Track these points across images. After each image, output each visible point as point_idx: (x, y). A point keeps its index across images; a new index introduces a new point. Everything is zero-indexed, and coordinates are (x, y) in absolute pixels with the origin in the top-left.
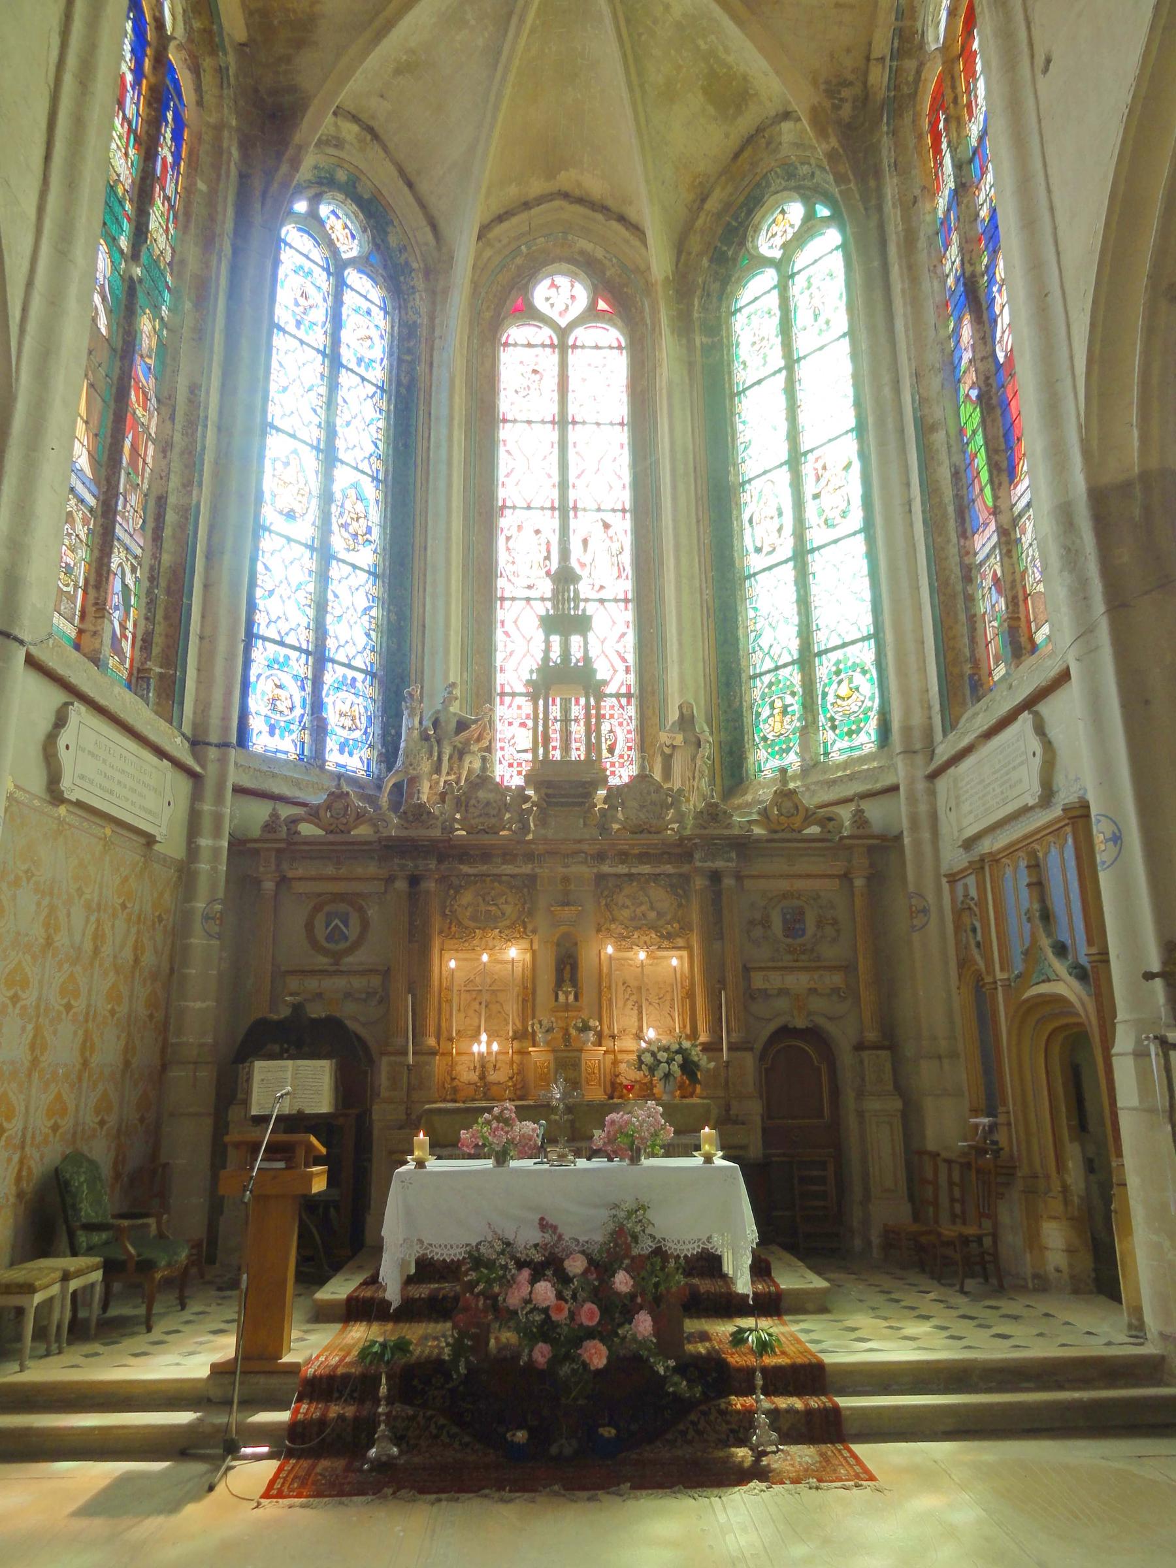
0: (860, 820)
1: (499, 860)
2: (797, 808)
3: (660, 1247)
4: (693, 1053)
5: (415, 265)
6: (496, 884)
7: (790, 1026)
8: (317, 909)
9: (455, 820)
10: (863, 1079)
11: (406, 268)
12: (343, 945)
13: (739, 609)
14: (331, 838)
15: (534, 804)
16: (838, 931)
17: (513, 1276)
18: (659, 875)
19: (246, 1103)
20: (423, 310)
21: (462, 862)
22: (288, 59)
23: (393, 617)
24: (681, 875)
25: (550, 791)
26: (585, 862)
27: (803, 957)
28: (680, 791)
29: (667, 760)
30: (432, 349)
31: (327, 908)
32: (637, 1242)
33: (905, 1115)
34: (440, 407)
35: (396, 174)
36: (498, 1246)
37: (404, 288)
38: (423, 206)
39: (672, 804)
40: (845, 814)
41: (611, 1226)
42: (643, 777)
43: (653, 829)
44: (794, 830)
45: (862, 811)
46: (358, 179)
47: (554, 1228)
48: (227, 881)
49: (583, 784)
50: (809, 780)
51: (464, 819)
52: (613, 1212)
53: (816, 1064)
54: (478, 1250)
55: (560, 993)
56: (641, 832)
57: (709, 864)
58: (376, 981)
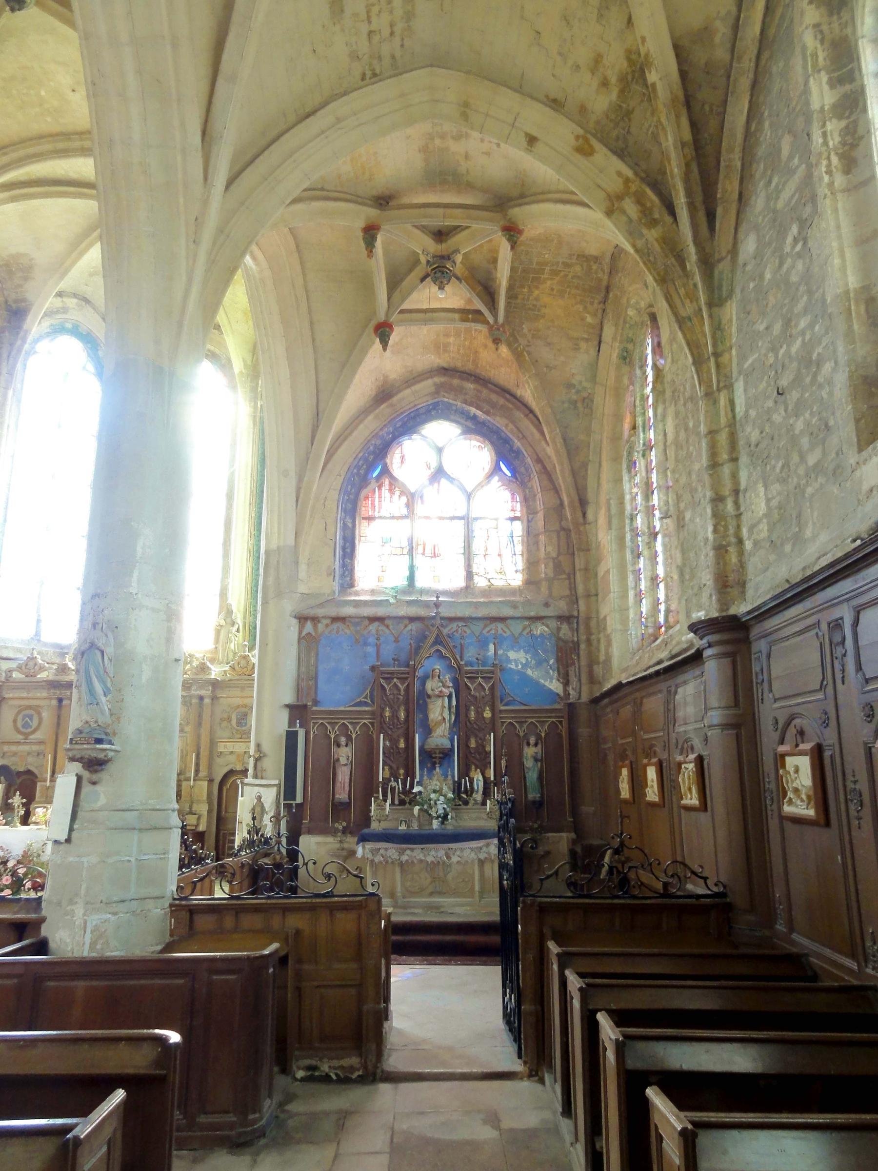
8: (19, 713)
12: (29, 730)
14: (28, 679)
22: (21, 286)
46: (78, 326)
57: (198, 693)
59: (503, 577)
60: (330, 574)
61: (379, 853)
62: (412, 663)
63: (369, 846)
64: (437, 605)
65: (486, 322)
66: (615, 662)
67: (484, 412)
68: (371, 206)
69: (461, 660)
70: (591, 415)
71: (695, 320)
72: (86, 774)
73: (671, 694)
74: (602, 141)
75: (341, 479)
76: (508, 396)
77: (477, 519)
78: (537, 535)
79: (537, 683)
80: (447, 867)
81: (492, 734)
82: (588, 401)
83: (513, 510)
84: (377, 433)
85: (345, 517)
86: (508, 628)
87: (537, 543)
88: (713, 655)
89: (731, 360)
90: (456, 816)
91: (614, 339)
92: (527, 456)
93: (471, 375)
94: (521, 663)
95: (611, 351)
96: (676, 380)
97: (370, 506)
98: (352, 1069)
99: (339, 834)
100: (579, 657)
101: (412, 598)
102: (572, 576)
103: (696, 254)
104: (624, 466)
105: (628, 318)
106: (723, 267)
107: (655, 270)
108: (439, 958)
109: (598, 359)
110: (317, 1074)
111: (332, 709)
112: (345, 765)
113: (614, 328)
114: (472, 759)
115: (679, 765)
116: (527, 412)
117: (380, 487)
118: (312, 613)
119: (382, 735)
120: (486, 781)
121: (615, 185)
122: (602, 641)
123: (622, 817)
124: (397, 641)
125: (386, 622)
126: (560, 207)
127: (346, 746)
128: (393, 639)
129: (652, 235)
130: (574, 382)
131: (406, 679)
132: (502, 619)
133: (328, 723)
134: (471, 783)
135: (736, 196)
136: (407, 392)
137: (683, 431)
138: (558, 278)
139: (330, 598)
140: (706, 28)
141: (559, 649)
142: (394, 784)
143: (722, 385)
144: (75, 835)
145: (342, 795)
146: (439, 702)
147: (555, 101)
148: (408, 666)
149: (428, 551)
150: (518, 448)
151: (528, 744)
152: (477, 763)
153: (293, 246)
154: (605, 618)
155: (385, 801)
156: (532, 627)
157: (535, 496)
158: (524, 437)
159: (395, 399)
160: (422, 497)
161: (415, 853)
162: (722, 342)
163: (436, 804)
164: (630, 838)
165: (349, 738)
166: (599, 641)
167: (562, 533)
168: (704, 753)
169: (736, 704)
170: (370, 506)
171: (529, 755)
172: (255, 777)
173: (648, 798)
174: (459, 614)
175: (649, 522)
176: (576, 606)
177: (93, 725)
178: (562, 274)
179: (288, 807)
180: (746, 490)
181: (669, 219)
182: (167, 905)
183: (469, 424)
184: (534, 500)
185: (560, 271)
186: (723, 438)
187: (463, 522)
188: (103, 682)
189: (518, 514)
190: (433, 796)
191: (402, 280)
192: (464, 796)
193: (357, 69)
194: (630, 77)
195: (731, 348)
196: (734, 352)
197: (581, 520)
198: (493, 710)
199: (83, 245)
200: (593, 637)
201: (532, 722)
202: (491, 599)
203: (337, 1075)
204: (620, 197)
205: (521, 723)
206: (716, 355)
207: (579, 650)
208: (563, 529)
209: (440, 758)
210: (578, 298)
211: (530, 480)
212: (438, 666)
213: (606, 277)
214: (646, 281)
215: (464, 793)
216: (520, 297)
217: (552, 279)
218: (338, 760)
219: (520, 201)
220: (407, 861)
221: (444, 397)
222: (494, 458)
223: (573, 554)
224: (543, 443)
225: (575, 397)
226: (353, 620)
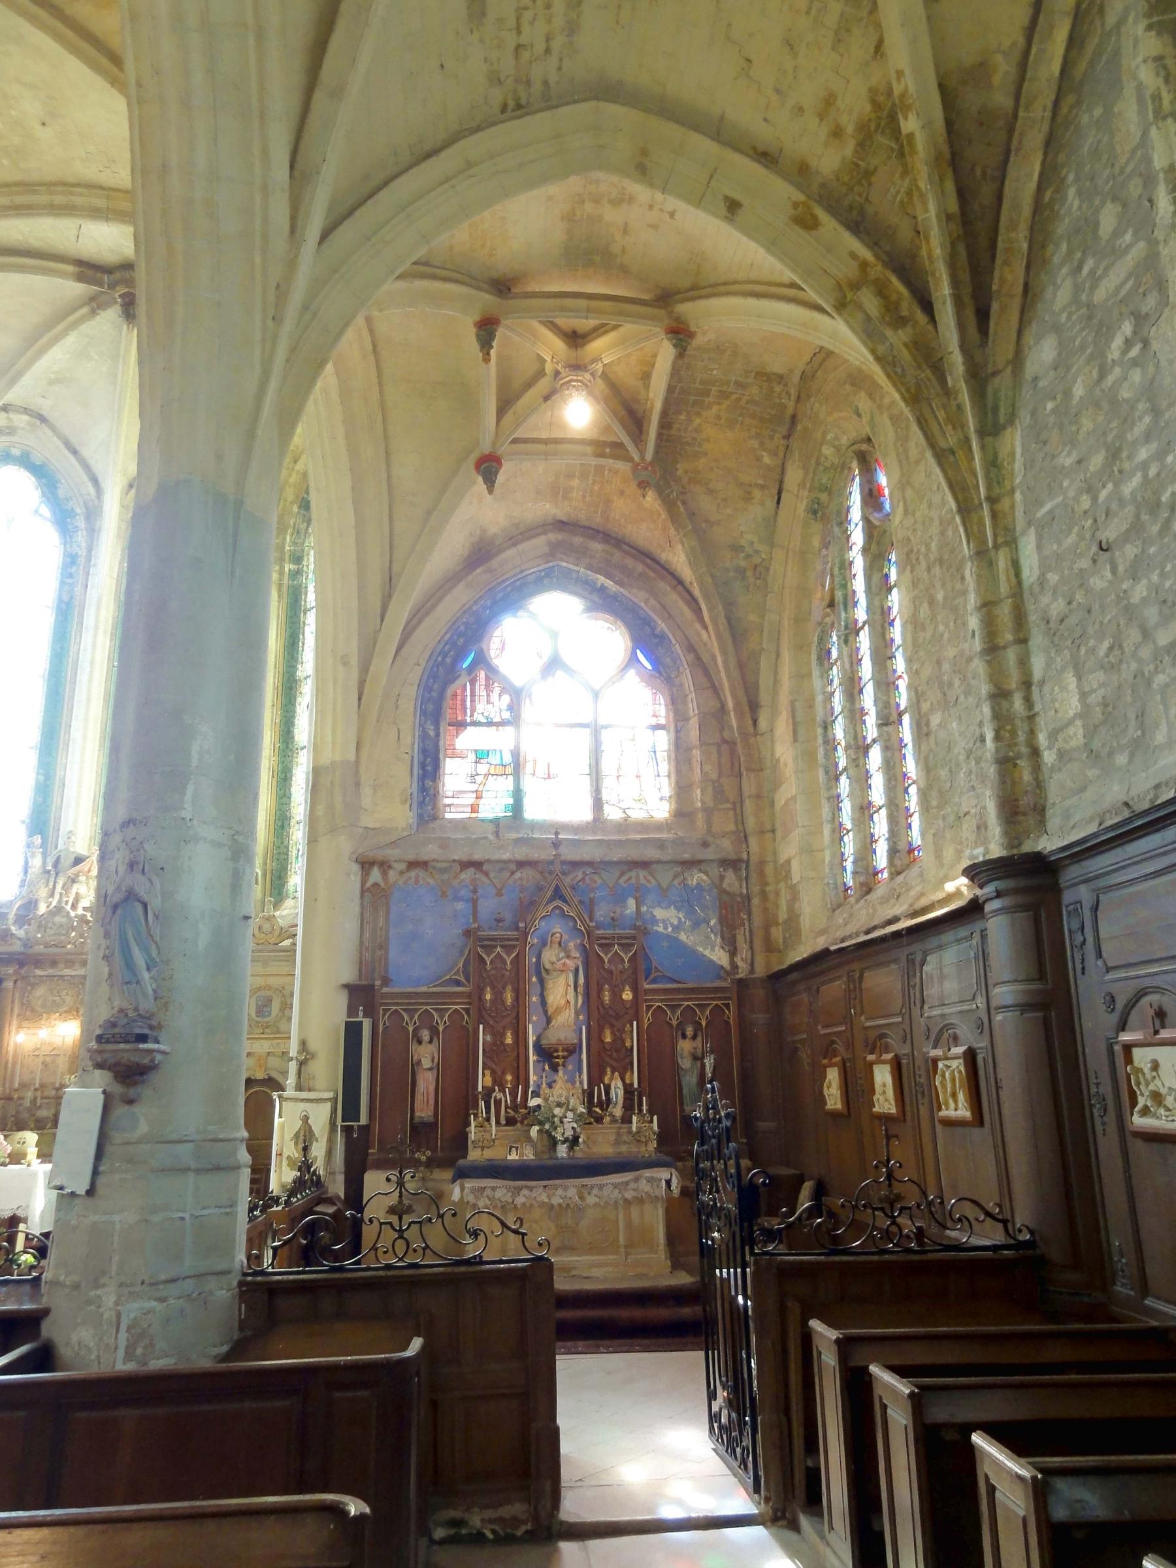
1: (63, 966)
5: (79, 511)
11: (72, 514)
13: (294, 772)
20: (83, 545)
21: (36, 968)
23: (41, 778)
27: (266, 1030)
30: (88, 574)
34: (89, 620)
35: (62, 447)
37: (70, 527)
38: (86, 467)
59: (644, 807)
60: (406, 801)
61: (485, 1194)
62: (521, 925)
63: (470, 1184)
64: (556, 844)
65: (629, 459)
66: (806, 922)
67: (616, 583)
68: (487, 292)
69: (591, 921)
70: (766, 586)
71: (960, 454)
72: (118, 1089)
73: (913, 967)
74: (832, 211)
75: (419, 671)
76: (648, 561)
77: (606, 727)
78: (690, 749)
79: (694, 952)
80: (580, 1210)
81: (635, 1023)
82: (761, 571)
83: (655, 716)
84: (470, 608)
85: (425, 722)
86: (654, 878)
87: (689, 761)
88: (1000, 909)
89: (1013, 507)
90: (588, 1138)
91: (802, 485)
92: (674, 642)
93: (598, 532)
94: (672, 925)
95: (796, 503)
96: (912, 538)
97: (459, 707)
98: (516, 1521)
99: (422, 1168)
100: (749, 914)
101: (520, 836)
102: (738, 805)
103: (964, 363)
104: (814, 657)
105: (823, 459)
106: (1001, 383)
107: (902, 383)
108: (580, 1343)
109: (776, 514)
110: (464, 1531)
111: (410, 990)
112: (430, 1069)
113: (801, 472)
114: (607, 1059)
115: (935, 1061)
116: (674, 583)
117: (473, 682)
118: (380, 855)
119: (481, 1026)
120: (628, 1090)
121: (849, 270)
122: (783, 892)
123: (888, 1137)
124: (499, 894)
125: (485, 867)
126: (752, 302)
127: (431, 1042)
128: (494, 891)
129: (898, 338)
130: (743, 542)
131: (515, 946)
132: (645, 865)
133: (404, 1010)
134: (607, 1093)
135: (1019, 289)
136: (511, 552)
137: (925, 605)
138: (728, 402)
139: (405, 834)
140: (981, 64)
141: (723, 906)
142: (499, 1095)
143: (1000, 540)
144: (102, 1180)
145: (424, 1110)
146: (561, 980)
147: (765, 154)
148: (517, 929)
149: (541, 771)
150: (662, 631)
151: (684, 1036)
152: (614, 1064)
153: (369, 346)
154: (788, 862)
155: (488, 1119)
156: (686, 874)
157: (686, 696)
158: (670, 616)
159: (494, 563)
160: (530, 696)
161: (534, 1194)
162: (998, 483)
163: (562, 1122)
164: (901, 1166)
165: (434, 1031)
166: (777, 893)
167: (725, 747)
168: (975, 1045)
169: (1041, 976)
170: (459, 707)
171: (686, 1053)
172: (299, 1088)
173: (876, 1109)
174: (587, 858)
175: (856, 731)
176: (744, 846)
177: (132, 1014)
178: (734, 397)
179: (347, 1130)
180: (1042, 683)
181: (921, 317)
182: (235, 1283)
183: (595, 597)
184: (685, 703)
185: (731, 393)
186: (1005, 612)
187: (588, 730)
188: (145, 950)
189: (663, 721)
190: (557, 1111)
191: (518, 397)
192: (598, 1110)
193: (497, 96)
194: (873, 126)
195: (1013, 491)
196: (1018, 496)
197: (751, 729)
198: (635, 990)
199: (45, 339)
200: (768, 889)
201: (659, 1006)
202: (629, 837)
203: (493, 1532)
204: (855, 286)
205: (673, 1008)
206: (992, 500)
207: (749, 905)
208: (725, 741)
209: (564, 1057)
210: (753, 430)
211: (677, 677)
212: (558, 928)
213: (791, 404)
214: (857, 408)
215: (597, 1107)
216: (676, 426)
217: (719, 404)
218: (419, 1062)
219: (691, 294)
220: (524, 1204)
221: (562, 560)
222: (629, 644)
223: (740, 775)
224: (698, 626)
225: (743, 563)
226: (439, 865)
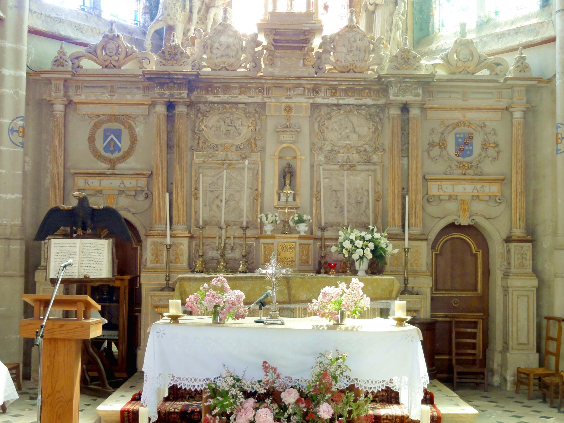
0: (522, 65)
1: (237, 91)
2: (472, 55)
3: (353, 385)
4: (383, 241)
6: (234, 110)
7: (456, 223)
8: (96, 126)
9: (202, 58)
10: (509, 263)
12: (117, 155)
15: (265, 48)
16: (498, 153)
17: (241, 403)
18: (361, 105)
19: (46, 268)
21: (208, 92)
24: (378, 106)
25: (278, 37)
26: (303, 95)
27: (469, 171)
28: (380, 39)
29: (371, 15)
31: (104, 126)
32: (336, 382)
33: (539, 290)
36: (231, 382)
39: (373, 50)
40: (511, 60)
41: (318, 370)
42: (351, 28)
43: (355, 70)
44: (469, 73)
45: (523, 59)
47: (275, 370)
48: (27, 104)
49: (304, 32)
50: (483, 34)
51: (209, 59)
52: (320, 359)
53: (474, 252)
54: (215, 383)
55: (282, 195)
56: (348, 72)
58: (142, 182)
